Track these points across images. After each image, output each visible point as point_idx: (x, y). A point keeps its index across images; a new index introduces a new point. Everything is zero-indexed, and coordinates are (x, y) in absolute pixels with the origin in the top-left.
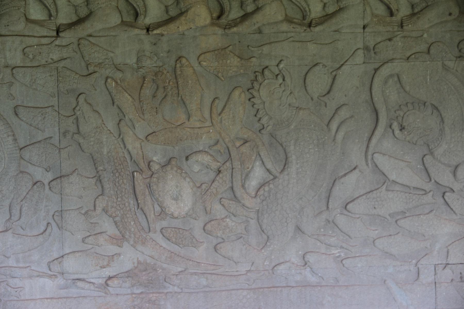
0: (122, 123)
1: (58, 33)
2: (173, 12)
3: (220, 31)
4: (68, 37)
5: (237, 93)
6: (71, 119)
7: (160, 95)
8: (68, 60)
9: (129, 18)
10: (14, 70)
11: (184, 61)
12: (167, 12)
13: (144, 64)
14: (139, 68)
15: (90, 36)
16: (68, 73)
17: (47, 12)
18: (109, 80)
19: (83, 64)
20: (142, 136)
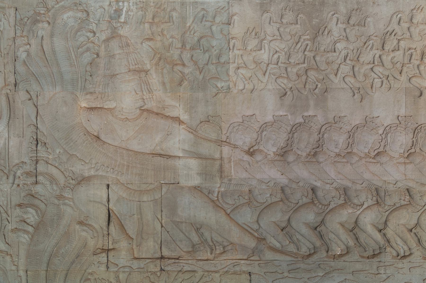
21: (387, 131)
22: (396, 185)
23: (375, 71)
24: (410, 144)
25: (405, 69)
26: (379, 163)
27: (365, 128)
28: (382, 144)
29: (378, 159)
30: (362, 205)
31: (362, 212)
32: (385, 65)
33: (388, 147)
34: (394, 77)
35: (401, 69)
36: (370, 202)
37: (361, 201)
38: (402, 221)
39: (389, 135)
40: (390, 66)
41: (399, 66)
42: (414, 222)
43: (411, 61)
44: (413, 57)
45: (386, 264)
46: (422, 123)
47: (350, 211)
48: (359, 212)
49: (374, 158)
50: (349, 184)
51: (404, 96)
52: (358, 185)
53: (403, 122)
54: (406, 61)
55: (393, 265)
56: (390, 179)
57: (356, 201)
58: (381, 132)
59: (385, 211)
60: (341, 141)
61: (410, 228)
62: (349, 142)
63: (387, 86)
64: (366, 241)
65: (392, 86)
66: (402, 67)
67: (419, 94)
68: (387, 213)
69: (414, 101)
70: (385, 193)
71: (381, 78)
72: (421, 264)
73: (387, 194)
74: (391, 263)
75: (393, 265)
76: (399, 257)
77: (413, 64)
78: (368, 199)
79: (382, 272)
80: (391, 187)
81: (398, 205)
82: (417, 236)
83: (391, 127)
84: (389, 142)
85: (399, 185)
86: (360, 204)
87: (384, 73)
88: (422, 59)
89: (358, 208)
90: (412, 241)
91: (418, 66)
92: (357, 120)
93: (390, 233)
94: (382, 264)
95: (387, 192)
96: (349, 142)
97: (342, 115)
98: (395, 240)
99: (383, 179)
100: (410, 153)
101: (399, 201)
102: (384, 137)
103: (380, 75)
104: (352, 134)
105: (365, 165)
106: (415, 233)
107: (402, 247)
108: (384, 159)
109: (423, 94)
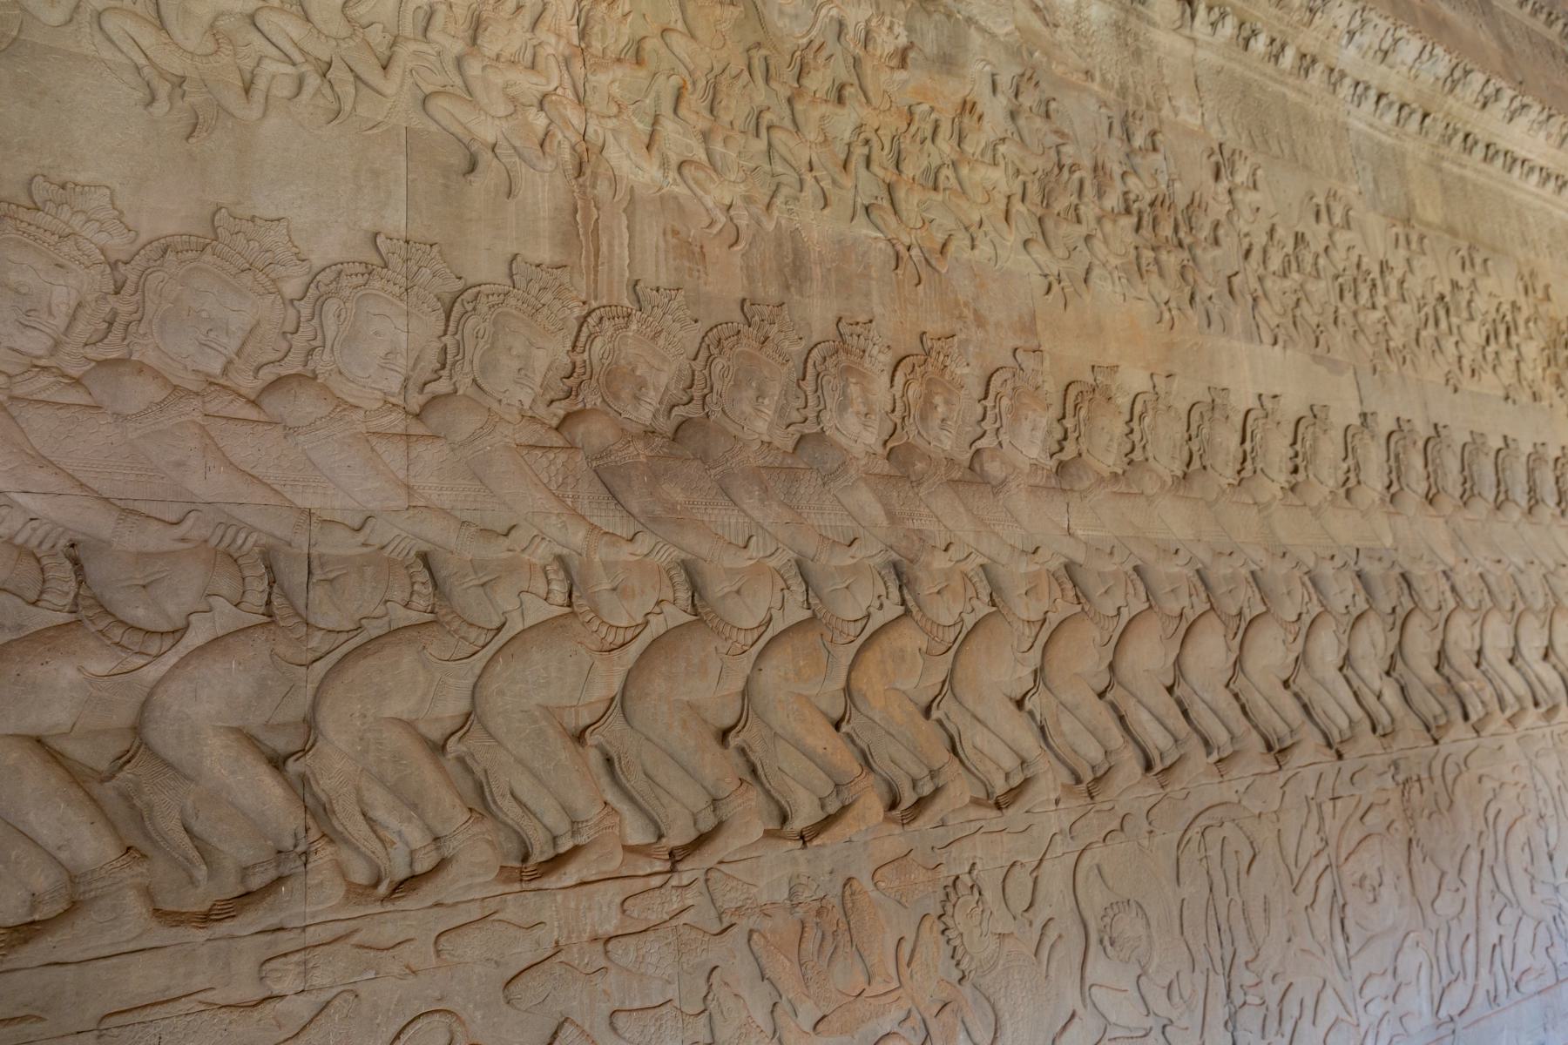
0: (779, 1010)
1: (674, 864)
2: (832, 808)
3: (897, 829)
4: (691, 869)
5: (927, 924)
6: (703, 1019)
7: (828, 949)
8: (692, 911)
9: (774, 825)
10: (610, 946)
11: (855, 883)
12: (823, 807)
13: (801, 899)
14: (794, 906)
15: (721, 862)
16: (693, 934)
17: (652, 829)
18: (755, 936)
19: (713, 913)
20: (808, 1027)
21: (323, 289)
22: (367, 530)
23: (265, 28)
24: (431, 360)
25: (404, 51)
26: (280, 427)
27: (208, 257)
28: (299, 342)
29: (276, 405)
30: (179, 633)
31: (176, 666)
32: (316, 18)
33: (326, 357)
34: (357, 77)
35: (387, 53)
36: (225, 617)
37: (171, 608)
38: (398, 707)
39: (332, 306)
40: (338, 27)
41: (376, 35)
42: (453, 707)
43: (432, 35)
44: (439, 20)
45: (312, 936)
46: (482, 277)
47: (98, 667)
48: (153, 672)
49: (254, 403)
50: (97, 522)
51: (402, 158)
52: (154, 526)
53: (395, 261)
54: (408, 30)
55: (347, 936)
56: (337, 504)
57: (140, 614)
58: (291, 288)
59: (311, 656)
60: (62, 296)
61: (436, 734)
62: (115, 313)
63: (322, 102)
64: (197, 827)
65: (347, 107)
66: (394, 44)
67: (465, 166)
68: (320, 668)
69: (447, 186)
70: (310, 573)
71: (294, 64)
72: (493, 905)
73: (318, 574)
74: (340, 928)
75: (347, 936)
76: (383, 889)
77: (438, 48)
78: (214, 601)
79: (286, 983)
80: (340, 545)
81: (374, 629)
82: (469, 770)
83: (340, 273)
84: (330, 335)
85: (381, 533)
86: (166, 627)
87: (308, 47)
88: (474, 39)
89: (154, 646)
90: (448, 798)
91: (459, 62)
92: (167, 212)
93: (334, 768)
94: (286, 942)
95: (322, 566)
96: (115, 313)
97: (81, 178)
98: (360, 801)
99: (299, 502)
100: (435, 398)
101: (380, 611)
102: (306, 312)
103: (288, 47)
104: (133, 278)
105: (202, 427)
106: (461, 760)
107: (400, 833)
108: (304, 406)
109: (480, 167)
